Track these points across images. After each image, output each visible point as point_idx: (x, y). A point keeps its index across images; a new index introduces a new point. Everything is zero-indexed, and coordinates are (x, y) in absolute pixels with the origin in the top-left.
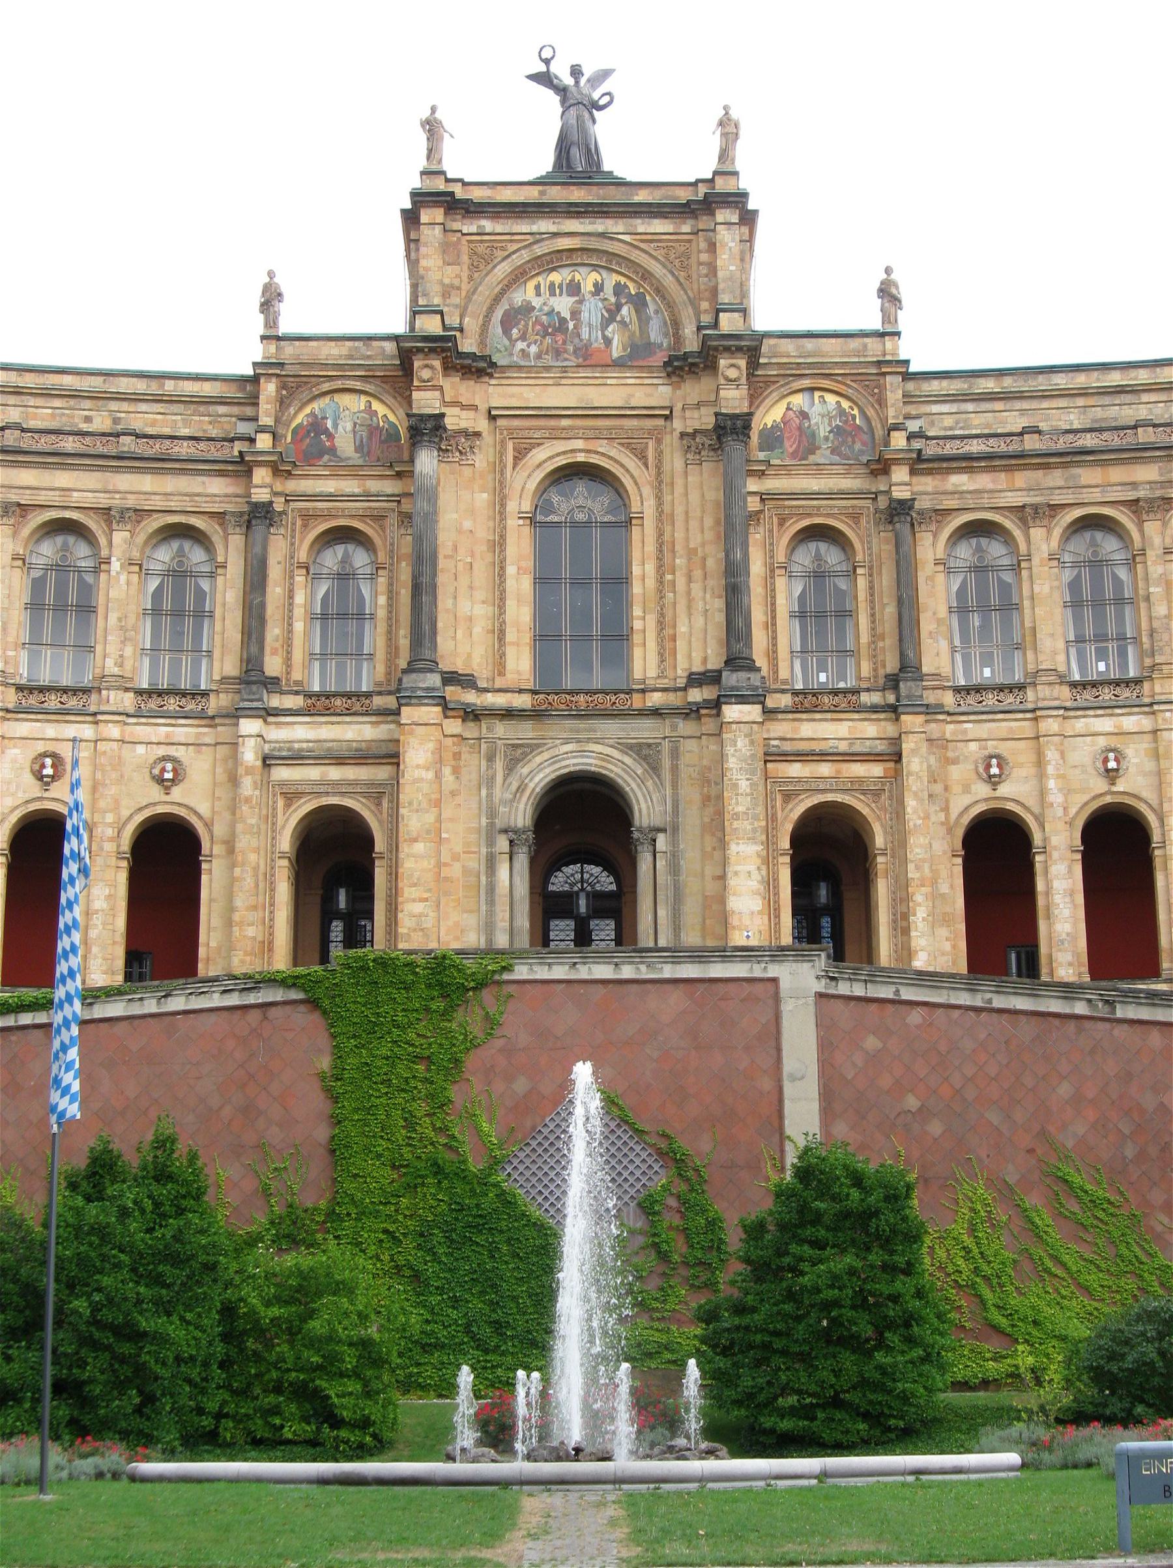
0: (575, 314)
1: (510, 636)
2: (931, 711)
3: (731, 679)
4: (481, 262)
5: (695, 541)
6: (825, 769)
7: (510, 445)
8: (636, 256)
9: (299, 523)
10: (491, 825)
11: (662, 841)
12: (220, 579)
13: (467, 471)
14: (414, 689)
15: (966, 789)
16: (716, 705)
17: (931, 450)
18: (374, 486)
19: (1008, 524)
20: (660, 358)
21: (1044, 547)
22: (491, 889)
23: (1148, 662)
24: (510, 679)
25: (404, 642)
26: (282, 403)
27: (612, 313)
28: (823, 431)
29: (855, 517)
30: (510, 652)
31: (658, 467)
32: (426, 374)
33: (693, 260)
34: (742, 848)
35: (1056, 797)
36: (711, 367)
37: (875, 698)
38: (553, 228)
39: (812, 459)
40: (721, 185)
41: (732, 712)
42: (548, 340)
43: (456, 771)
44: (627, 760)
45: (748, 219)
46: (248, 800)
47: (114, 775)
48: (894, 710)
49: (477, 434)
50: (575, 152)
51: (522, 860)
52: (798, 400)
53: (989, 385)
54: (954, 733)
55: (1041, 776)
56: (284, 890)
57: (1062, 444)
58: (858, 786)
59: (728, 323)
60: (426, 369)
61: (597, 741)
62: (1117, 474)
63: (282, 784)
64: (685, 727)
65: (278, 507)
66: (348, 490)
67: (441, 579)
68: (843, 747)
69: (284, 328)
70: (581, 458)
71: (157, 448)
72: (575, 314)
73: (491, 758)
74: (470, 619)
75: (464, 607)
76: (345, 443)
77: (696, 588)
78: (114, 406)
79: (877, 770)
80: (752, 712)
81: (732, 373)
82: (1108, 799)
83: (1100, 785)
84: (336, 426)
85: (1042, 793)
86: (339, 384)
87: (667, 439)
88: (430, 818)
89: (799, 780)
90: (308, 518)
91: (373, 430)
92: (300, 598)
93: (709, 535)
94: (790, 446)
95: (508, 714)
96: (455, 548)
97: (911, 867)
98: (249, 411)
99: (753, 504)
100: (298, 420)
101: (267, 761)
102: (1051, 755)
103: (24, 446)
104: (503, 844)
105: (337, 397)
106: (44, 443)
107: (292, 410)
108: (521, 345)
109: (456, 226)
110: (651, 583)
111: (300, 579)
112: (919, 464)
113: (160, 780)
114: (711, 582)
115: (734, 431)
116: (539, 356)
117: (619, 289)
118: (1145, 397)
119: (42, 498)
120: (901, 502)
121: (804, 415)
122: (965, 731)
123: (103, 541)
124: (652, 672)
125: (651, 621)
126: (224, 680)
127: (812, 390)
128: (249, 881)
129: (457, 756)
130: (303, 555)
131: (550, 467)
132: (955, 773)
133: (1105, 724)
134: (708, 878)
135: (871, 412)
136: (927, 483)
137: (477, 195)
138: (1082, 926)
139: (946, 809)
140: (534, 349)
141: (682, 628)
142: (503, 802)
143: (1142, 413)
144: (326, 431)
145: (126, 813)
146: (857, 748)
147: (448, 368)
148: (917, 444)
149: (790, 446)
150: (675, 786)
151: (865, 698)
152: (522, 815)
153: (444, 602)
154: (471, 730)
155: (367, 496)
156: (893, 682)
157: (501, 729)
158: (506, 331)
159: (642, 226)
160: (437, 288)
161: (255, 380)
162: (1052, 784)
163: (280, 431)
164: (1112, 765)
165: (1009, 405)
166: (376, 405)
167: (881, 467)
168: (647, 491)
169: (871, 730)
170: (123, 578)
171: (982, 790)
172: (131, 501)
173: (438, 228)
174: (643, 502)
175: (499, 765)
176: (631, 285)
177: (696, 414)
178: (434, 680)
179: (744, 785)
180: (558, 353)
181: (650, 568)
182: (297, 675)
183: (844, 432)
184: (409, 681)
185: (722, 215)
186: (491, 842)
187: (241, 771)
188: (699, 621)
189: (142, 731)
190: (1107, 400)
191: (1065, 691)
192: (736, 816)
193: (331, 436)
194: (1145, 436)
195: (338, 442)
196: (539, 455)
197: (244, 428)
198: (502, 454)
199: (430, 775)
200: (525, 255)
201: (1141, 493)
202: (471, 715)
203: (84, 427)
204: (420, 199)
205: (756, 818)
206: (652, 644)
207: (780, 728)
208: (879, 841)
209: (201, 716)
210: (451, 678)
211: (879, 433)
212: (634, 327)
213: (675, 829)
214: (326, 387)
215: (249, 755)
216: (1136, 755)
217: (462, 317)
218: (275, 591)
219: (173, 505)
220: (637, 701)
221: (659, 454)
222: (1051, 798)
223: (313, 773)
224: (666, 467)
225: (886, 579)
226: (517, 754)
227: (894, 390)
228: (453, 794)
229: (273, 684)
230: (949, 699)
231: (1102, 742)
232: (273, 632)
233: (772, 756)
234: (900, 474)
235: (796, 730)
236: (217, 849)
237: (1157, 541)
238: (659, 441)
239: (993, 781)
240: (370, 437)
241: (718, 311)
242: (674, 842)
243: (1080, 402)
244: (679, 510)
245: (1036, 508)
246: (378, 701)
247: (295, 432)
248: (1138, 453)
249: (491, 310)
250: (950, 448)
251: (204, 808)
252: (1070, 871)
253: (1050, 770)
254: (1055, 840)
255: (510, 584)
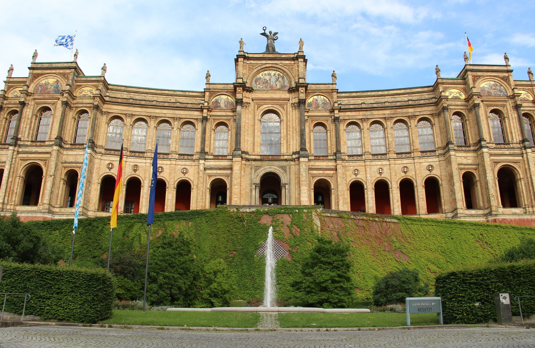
0: (270, 80)
1: (256, 144)
2: (343, 160)
3: (301, 153)
4: (251, 69)
5: (294, 125)
6: (321, 172)
7: (256, 106)
8: (282, 68)
9: (213, 121)
10: (251, 183)
11: (287, 186)
12: (196, 132)
13: (247, 111)
14: (236, 154)
15: (350, 176)
16: (298, 158)
17: (343, 107)
18: (228, 114)
19: (359, 122)
20: (287, 88)
21: (366, 127)
22: (251, 196)
23: (388, 150)
24: (255, 153)
25: (234, 145)
26: (210, 97)
27: (277, 80)
28: (320, 103)
29: (327, 121)
30: (256, 147)
31: (287, 110)
32: (239, 91)
33: (294, 69)
34: (304, 188)
35: (369, 178)
36: (298, 90)
37: (332, 157)
38: (266, 63)
39: (318, 109)
40: (300, 54)
41: (302, 159)
42: (264, 85)
43: (244, 171)
44: (280, 170)
45: (305, 61)
46: (201, 177)
47: (174, 171)
48: (336, 160)
49: (250, 103)
50: (270, 48)
51: (258, 190)
52: (315, 97)
53: (354, 94)
54: (348, 165)
55: (366, 174)
56: (208, 196)
57: (370, 106)
58: (328, 175)
59: (301, 81)
60: (239, 90)
61: (273, 165)
62: (381, 112)
63: (208, 174)
64: (292, 163)
65: (209, 117)
66: (223, 114)
67: (242, 132)
68: (325, 167)
69: (211, 82)
70: (271, 108)
71: (184, 105)
72: (270, 80)
73: (251, 169)
74: (248, 140)
75: (246, 138)
76: (222, 105)
77: (294, 135)
78: (176, 97)
79: (332, 172)
80: (306, 159)
81: (302, 91)
82: (380, 178)
83: (379, 175)
84: (221, 102)
85: (366, 177)
86: (221, 93)
87: (288, 105)
88: (239, 181)
89: (316, 174)
90: (214, 120)
91: (228, 102)
92: (212, 136)
93: (297, 124)
94: (314, 106)
95: (255, 160)
96: (245, 126)
97: (339, 192)
98: (203, 99)
99: (306, 118)
100: (213, 100)
101: (205, 169)
102: (368, 169)
103: (157, 105)
104: (254, 186)
105: (221, 96)
106: (161, 104)
107: (212, 98)
108: (259, 86)
109: (246, 62)
110: (285, 134)
111: (213, 132)
112: (340, 110)
113: (183, 173)
114: (297, 133)
115: (302, 103)
116: (262, 88)
117: (279, 75)
118: (387, 97)
119: (160, 115)
120: (337, 117)
121: (317, 100)
122: (350, 164)
123: (173, 124)
124: (285, 152)
125: (285, 141)
126: (197, 152)
127: (318, 95)
128: (201, 193)
129: (244, 168)
130: (213, 127)
131: (264, 110)
132: (348, 173)
133: (379, 163)
134: (297, 194)
135: (330, 100)
136: (342, 114)
137: (250, 56)
138: (375, 205)
139: (346, 180)
140: (261, 86)
141: (292, 143)
142: (254, 178)
143: (386, 100)
144: (219, 103)
145: (176, 179)
146: (328, 168)
147: (244, 90)
148: (340, 106)
149: (314, 106)
150: (290, 175)
151: (329, 157)
152: (258, 181)
153: (242, 137)
154: (248, 163)
155: (227, 116)
156: (335, 154)
157: (253, 163)
158: (256, 83)
159: (283, 62)
160: (242, 74)
161: (204, 92)
162: (368, 175)
163: (209, 102)
164: (381, 171)
165: (359, 98)
166: (229, 97)
167: (332, 111)
168: (284, 115)
169: (331, 164)
170: (177, 131)
171: (354, 176)
172: (179, 116)
173: (242, 62)
174: (283, 117)
175: (253, 170)
176: (281, 74)
177: (294, 100)
178: (240, 152)
179: (304, 175)
180: (266, 87)
181: (285, 130)
182: (212, 152)
183: (324, 103)
184: (235, 152)
185: (300, 60)
186: (251, 186)
187: (200, 171)
188: (295, 141)
189: (179, 162)
190: (379, 98)
191: (371, 156)
192: (303, 181)
193: (219, 103)
194: (387, 104)
195: (221, 105)
196: (262, 107)
197: (202, 102)
198: (254, 107)
199: (239, 172)
200: (260, 68)
201: (386, 116)
202: (248, 160)
203: (170, 101)
204: (238, 56)
205: (307, 181)
206: (285, 146)
207: (312, 163)
208: (332, 187)
209: (192, 160)
210: (243, 152)
211: (332, 104)
212: (282, 82)
213: (290, 184)
214: (219, 94)
215: (202, 168)
216: (386, 169)
217: (247, 80)
218: (207, 134)
219: (187, 117)
220: (282, 158)
221: (287, 108)
222: (368, 178)
223: (215, 172)
224: (288, 110)
225: (333, 133)
226: (257, 168)
227: (335, 95)
228: (244, 176)
229: (206, 153)
230: (347, 158)
231: (379, 167)
232: (207, 143)
233: (310, 169)
234: (336, 112)
235: (315, 164)
236: (195, 187)
237: (389, 126)
238: (287, 105)
239: (356, 175)
240: (228, 104)
241: (299, 79)
242: (290, 187)
243: (373, 98)
244: (291, 119)
245: (364, 119)
246: (228, 157)
247: (212, 103)
248: (385, 108)
249: (253, 79)
250: (347, 107)
251: (192, 179)
252: (372, 193)
253: (368, 172)
254: (369, 187)
255: (256, 133)
